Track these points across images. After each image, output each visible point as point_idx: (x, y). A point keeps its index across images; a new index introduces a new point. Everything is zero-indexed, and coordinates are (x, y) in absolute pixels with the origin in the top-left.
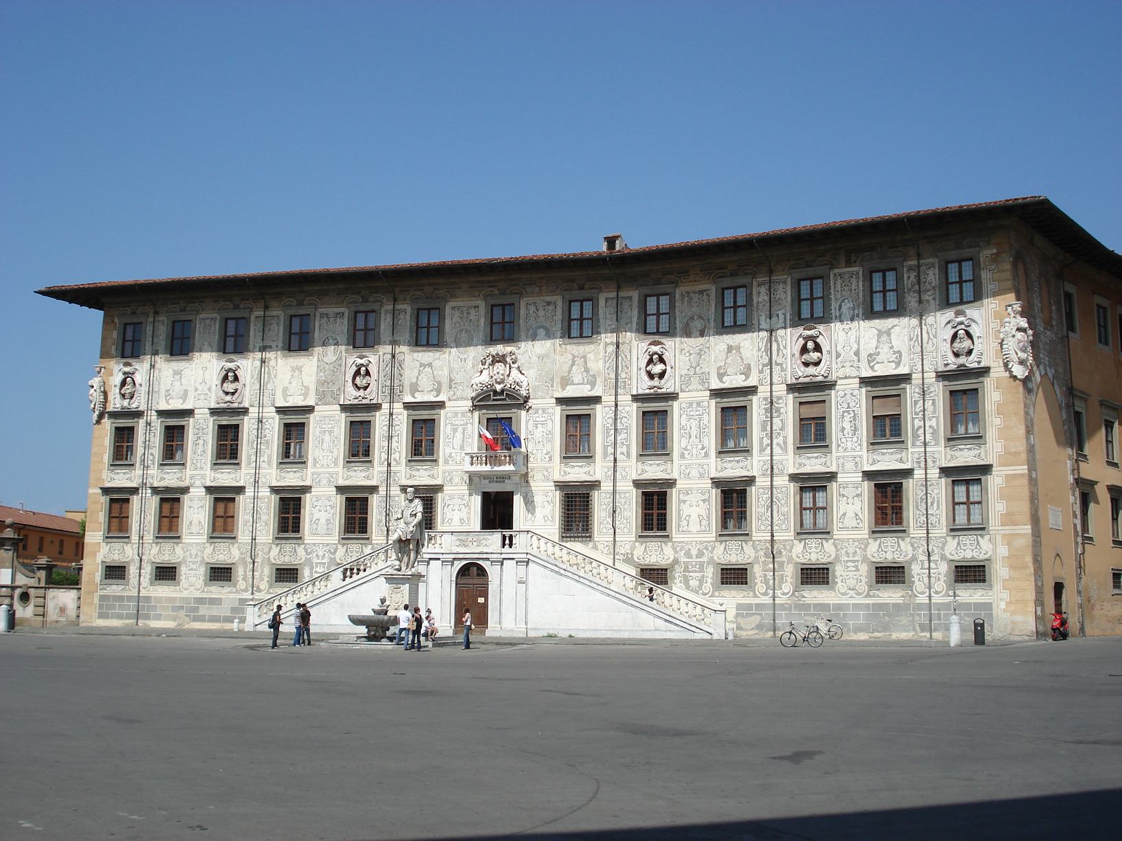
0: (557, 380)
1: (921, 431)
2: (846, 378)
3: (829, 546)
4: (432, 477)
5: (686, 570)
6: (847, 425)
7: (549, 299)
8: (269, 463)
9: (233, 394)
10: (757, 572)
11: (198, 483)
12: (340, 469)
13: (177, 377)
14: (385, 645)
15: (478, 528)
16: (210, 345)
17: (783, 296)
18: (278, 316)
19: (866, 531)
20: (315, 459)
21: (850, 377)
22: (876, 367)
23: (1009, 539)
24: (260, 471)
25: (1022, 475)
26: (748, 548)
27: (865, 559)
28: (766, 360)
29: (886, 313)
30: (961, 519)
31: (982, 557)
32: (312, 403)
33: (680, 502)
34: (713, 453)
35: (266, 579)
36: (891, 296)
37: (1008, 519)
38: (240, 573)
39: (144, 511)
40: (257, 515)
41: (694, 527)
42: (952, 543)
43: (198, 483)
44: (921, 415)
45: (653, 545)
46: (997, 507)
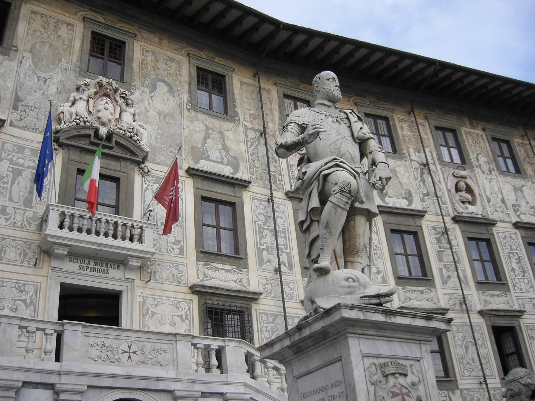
6: (515, 266)
7: (169, 54)
22: (522, 216)
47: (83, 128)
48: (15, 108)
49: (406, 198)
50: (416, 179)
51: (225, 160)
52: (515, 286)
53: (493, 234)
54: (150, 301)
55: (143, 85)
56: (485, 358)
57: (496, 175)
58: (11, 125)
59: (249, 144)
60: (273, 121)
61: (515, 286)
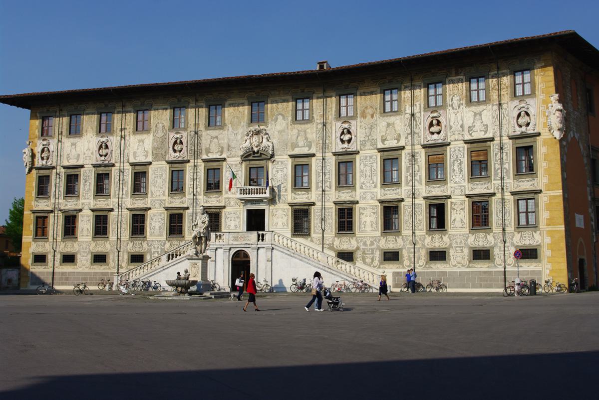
0: (289, 144)
1: (499, 171)
2: (455, 140)
3: (446, 238)
4: (218, 201)
5: (364, 253)
6: (456, 168)
8: (127, 195)
9: (105, 156)
10: (405, 255)
11: (86, 207)
12: (166, 198)
13: (74, 147)
14: (186, 297)
15: (245, 230)
16: (92, 128)
17: (419, 94)
19: (468, 229)
20: (152, 192)
21: (457, 140)
22: (473, 134)
23: (551, 234)
24: (121, 201)
25: (560, 196)
26: (399, 240)
27: (467, 245)
28: (409, 131)
29: (479, 103)
30: (523, 222)
31: (535, 244)
32: (150, 160)
33: (361, 214)
34: (379, 185)
35: (126, 261)
36: (482, 93)
37: (551, 222)
38: (112, 258)
39: (55, 225)
40: (119, 225)
41: (368, 228)
42: (517, 236)
43: (86, 207)
44: (499, 162)
45: (345, 239)
46: (544, 215)
47: (249, 152)
48: (228, 150)
49: (397, 139)
50: (405, 125)
51: (306, 144)
52: (451, 180)
53: (446, 151)
54: (274, 211)
55: (272, 121)
56: (420, 221)
57: (463, 108)
58: (228, 157)
59: (318, 132)
60: (331, 115)
61: (451, 180)
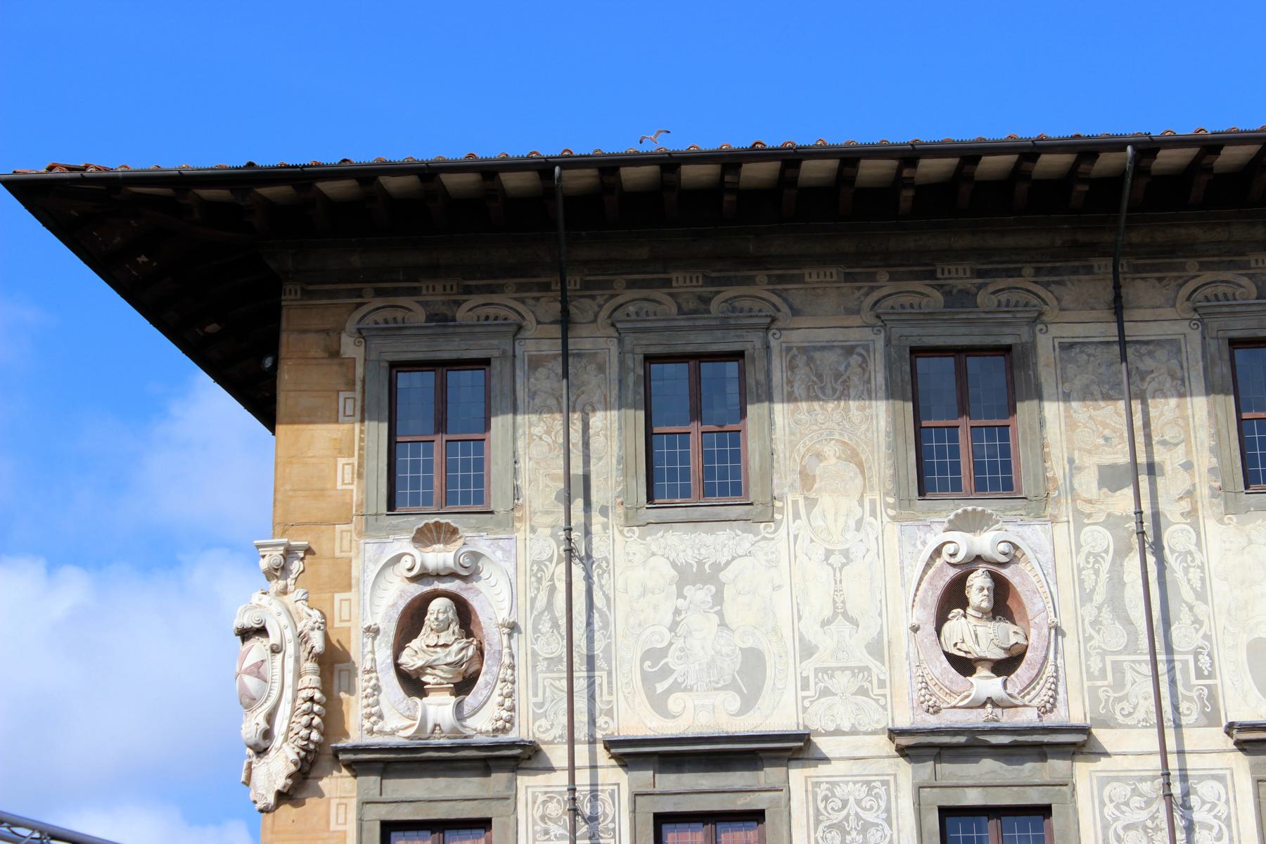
9: (1006, 666)
13: (700, 594)
16: (852, 456)
18: (1174, 346)
